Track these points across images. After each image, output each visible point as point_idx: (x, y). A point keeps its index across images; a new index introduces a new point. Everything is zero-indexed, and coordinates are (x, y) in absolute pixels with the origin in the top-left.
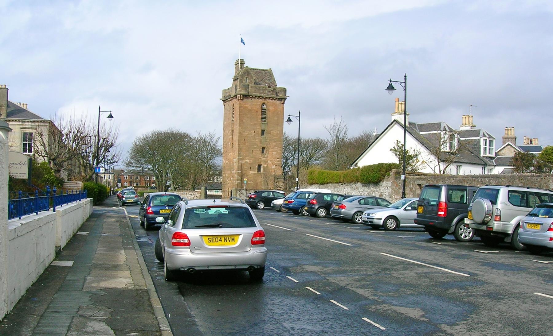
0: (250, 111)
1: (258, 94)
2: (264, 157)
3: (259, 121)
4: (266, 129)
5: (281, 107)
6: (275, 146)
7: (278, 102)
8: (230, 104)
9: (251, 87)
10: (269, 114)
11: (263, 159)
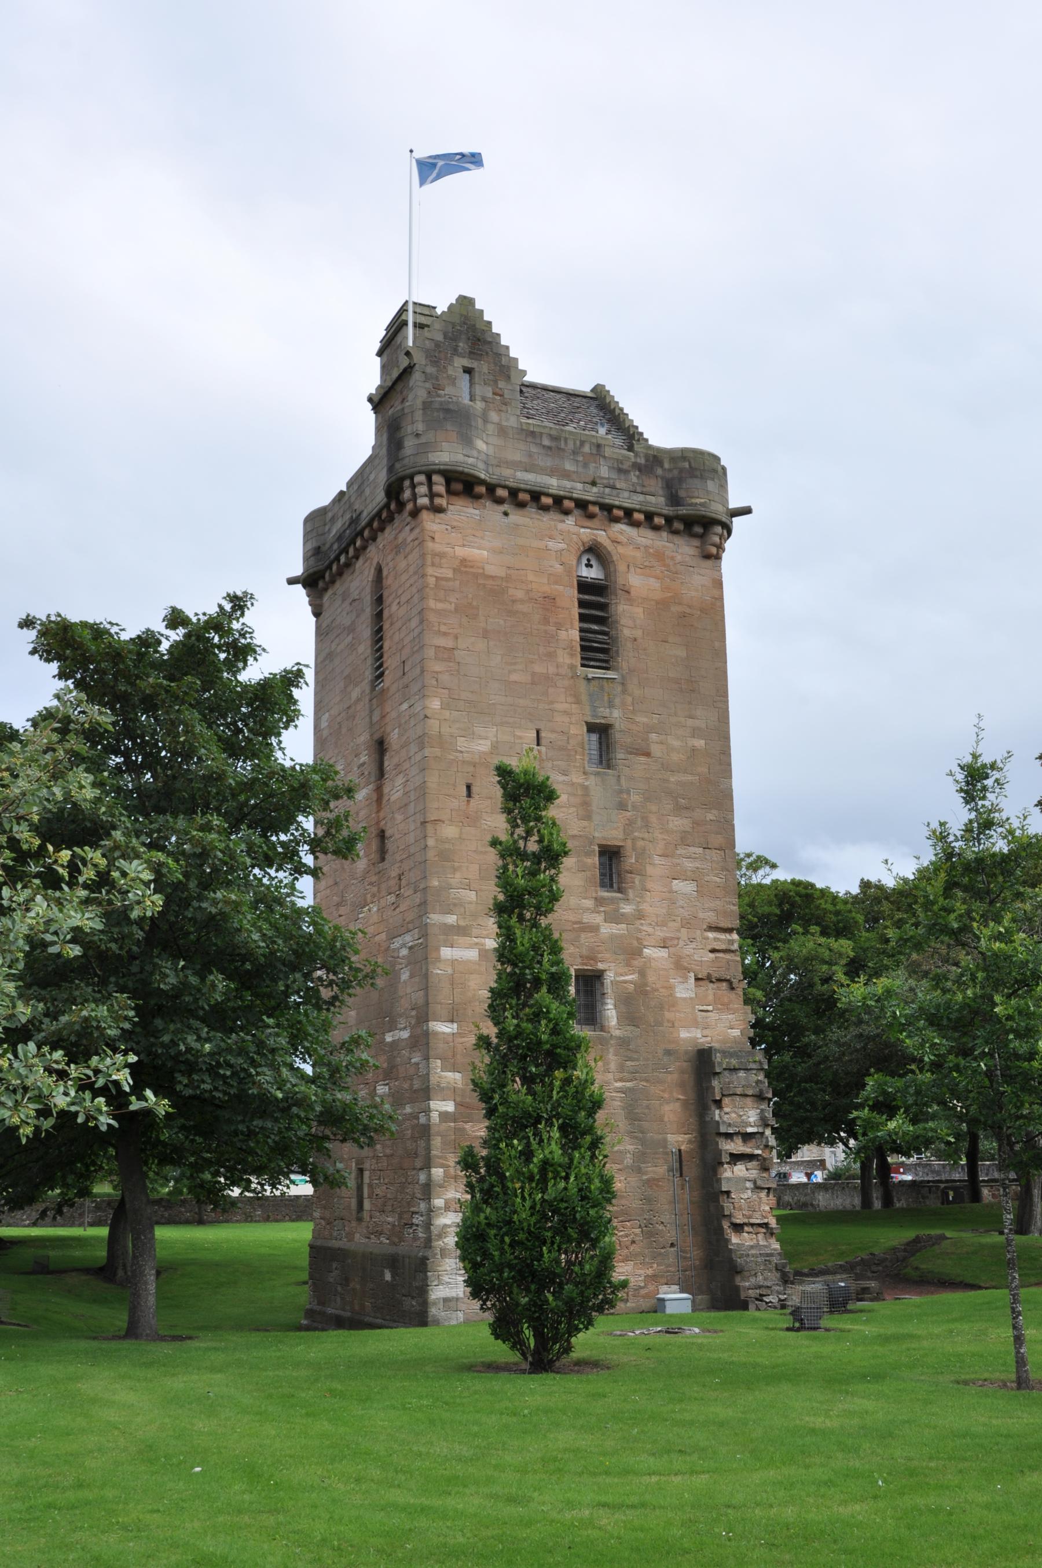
0: (495, 591)
1: (553, 484)
2: (615, 918)
3: (569, 658)
4: (615, 716)
5: (698, 579)
6: (684, 840)
7: (683, 549)
8: (358, 582)
9: (502, 431)
10: (630, 618)
11: (608, 929)
